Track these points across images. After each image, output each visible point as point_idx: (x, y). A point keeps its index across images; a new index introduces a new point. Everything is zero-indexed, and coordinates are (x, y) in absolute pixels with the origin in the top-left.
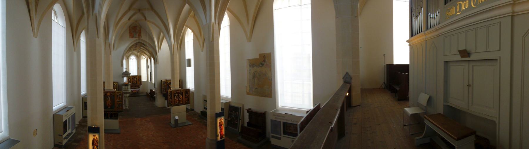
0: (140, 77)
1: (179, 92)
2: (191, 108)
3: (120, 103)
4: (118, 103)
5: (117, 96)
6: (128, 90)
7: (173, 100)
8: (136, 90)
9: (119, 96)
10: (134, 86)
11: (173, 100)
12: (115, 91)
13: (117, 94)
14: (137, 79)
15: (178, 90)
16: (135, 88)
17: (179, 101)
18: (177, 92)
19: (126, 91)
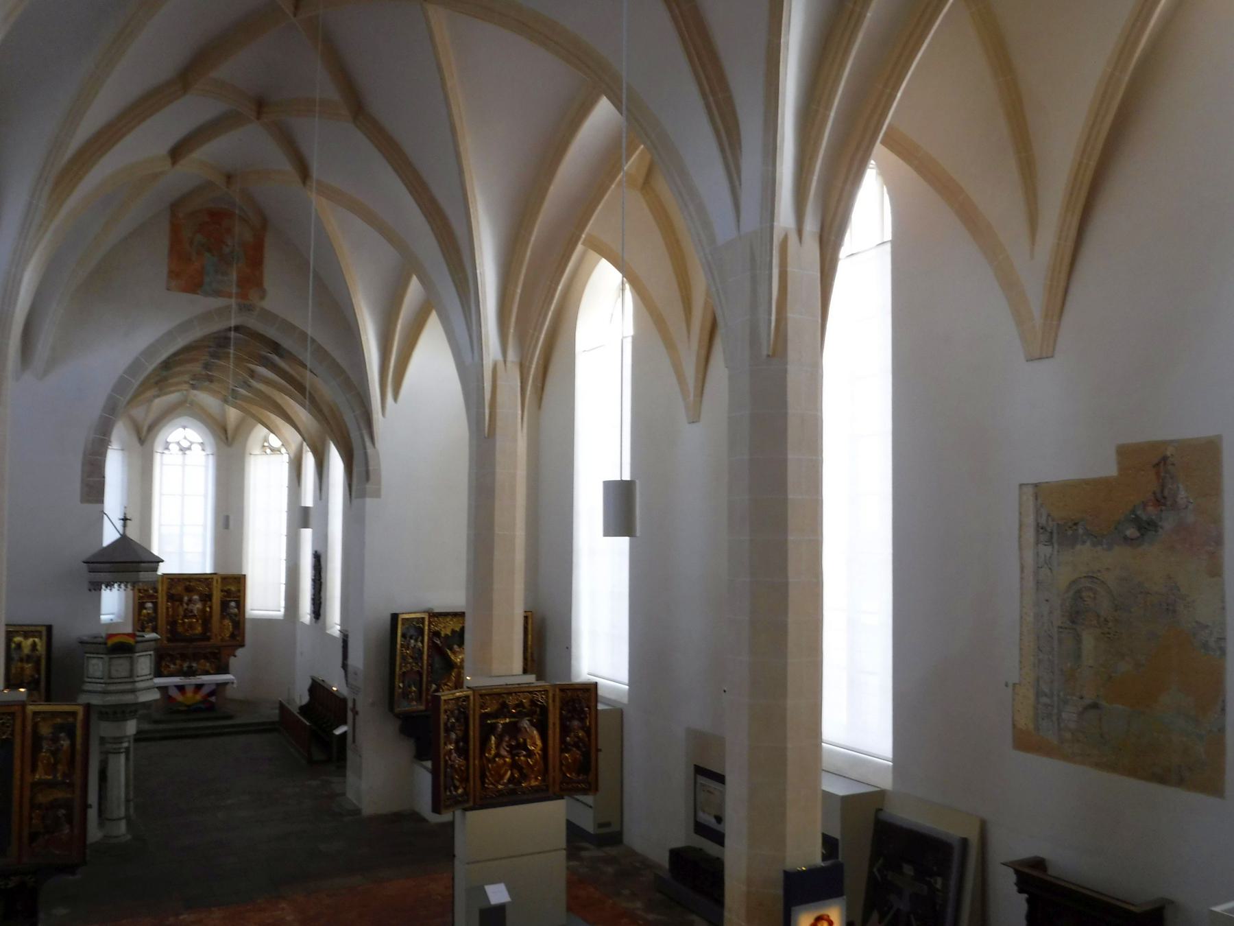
0: (233, 589)
1: (520, 705)
2: (601, 825)
3: (60, 794)
4: (41, 798)
5: (37, 739)
6: (133, 691)
7: (475, 762)
8: (199, 687)
9: (55, 739)
10: (184, 657)
11: (475, 762)
12: (23, 705)
13: (35, 726)
14: (206, 598)
15: (510, 691)
16: (191, 673)
17: (520, 769)
18: (504, 705)
19: (112, 699)
